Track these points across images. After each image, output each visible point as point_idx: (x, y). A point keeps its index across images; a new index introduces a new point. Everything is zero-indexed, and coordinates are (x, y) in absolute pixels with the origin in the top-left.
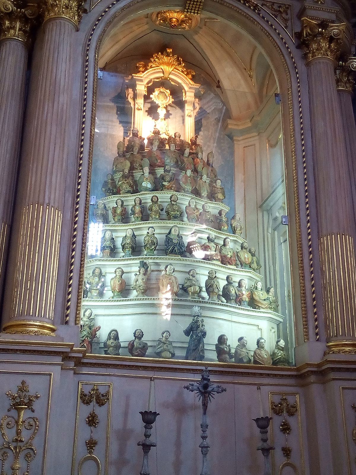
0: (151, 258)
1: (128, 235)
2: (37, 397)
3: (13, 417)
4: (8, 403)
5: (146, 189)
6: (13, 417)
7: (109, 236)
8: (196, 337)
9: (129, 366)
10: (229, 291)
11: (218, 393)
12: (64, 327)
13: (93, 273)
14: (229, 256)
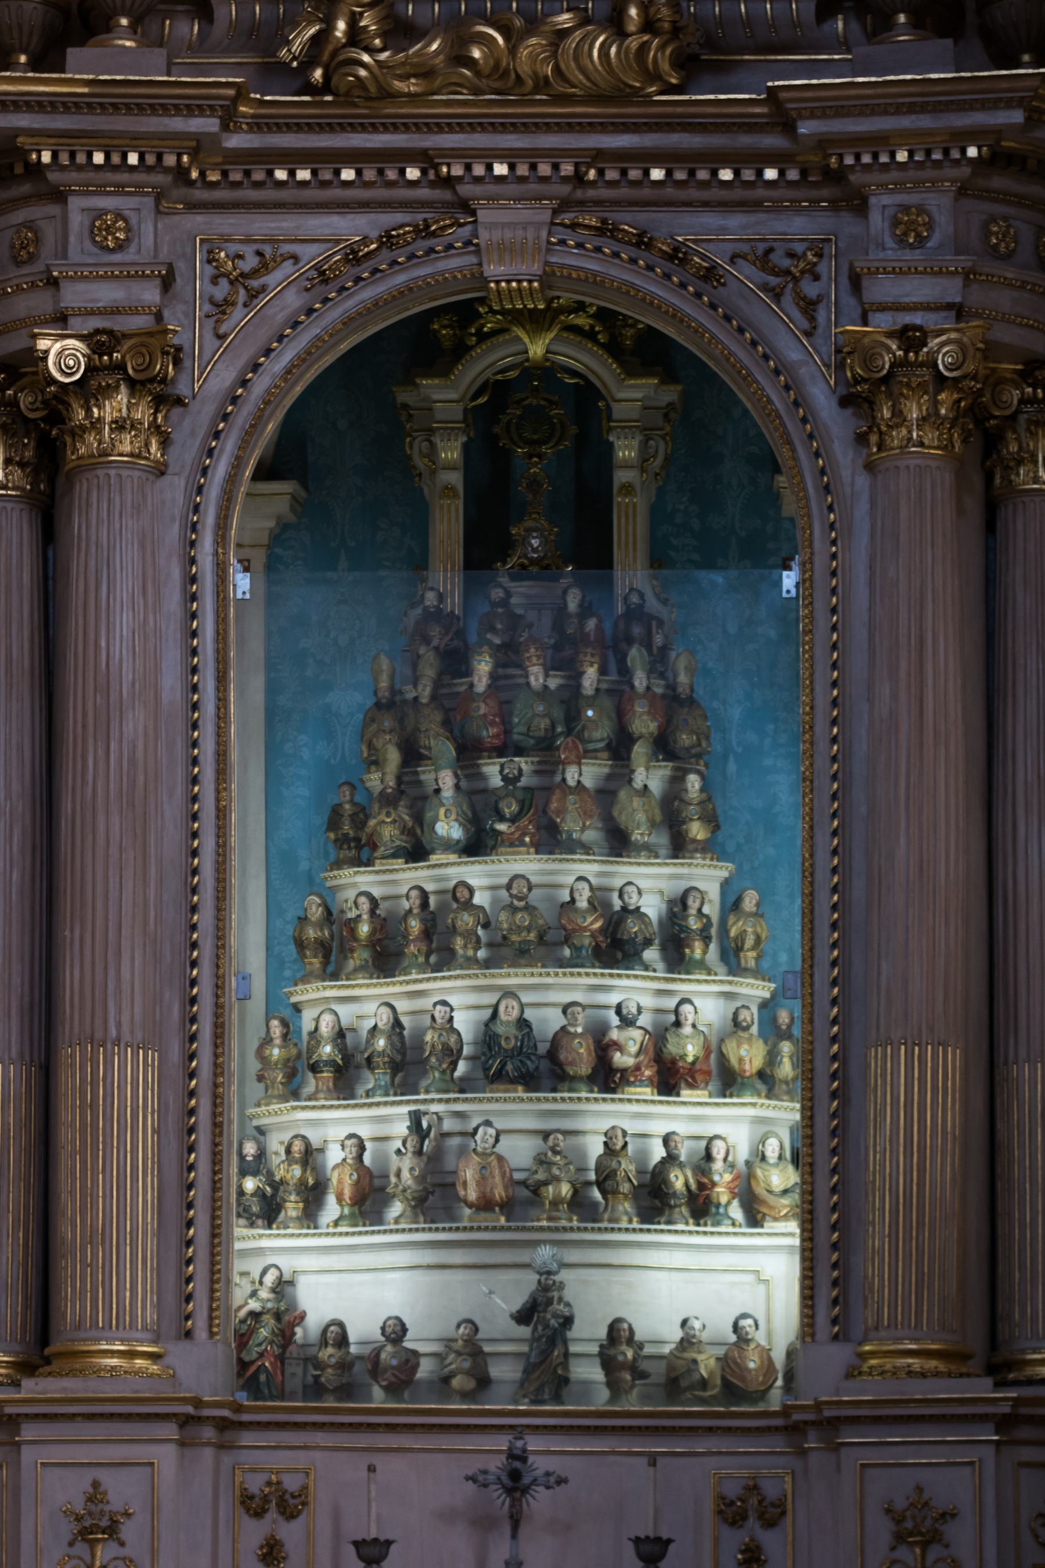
0: (440, 1101)
1: (380, 1025)
2: (127, 1515)
3: (80, 1558)
4: (67, 1528)
5: (449, 846)
6: (80, 1558)
7: (330, 1029)
8: (544, 1330)
9: (351, 1425)
10: (666, 1182)
11: (548, 1487)
12: (184, 1345)
13: (288, 1151)
14: (690, 1059)
